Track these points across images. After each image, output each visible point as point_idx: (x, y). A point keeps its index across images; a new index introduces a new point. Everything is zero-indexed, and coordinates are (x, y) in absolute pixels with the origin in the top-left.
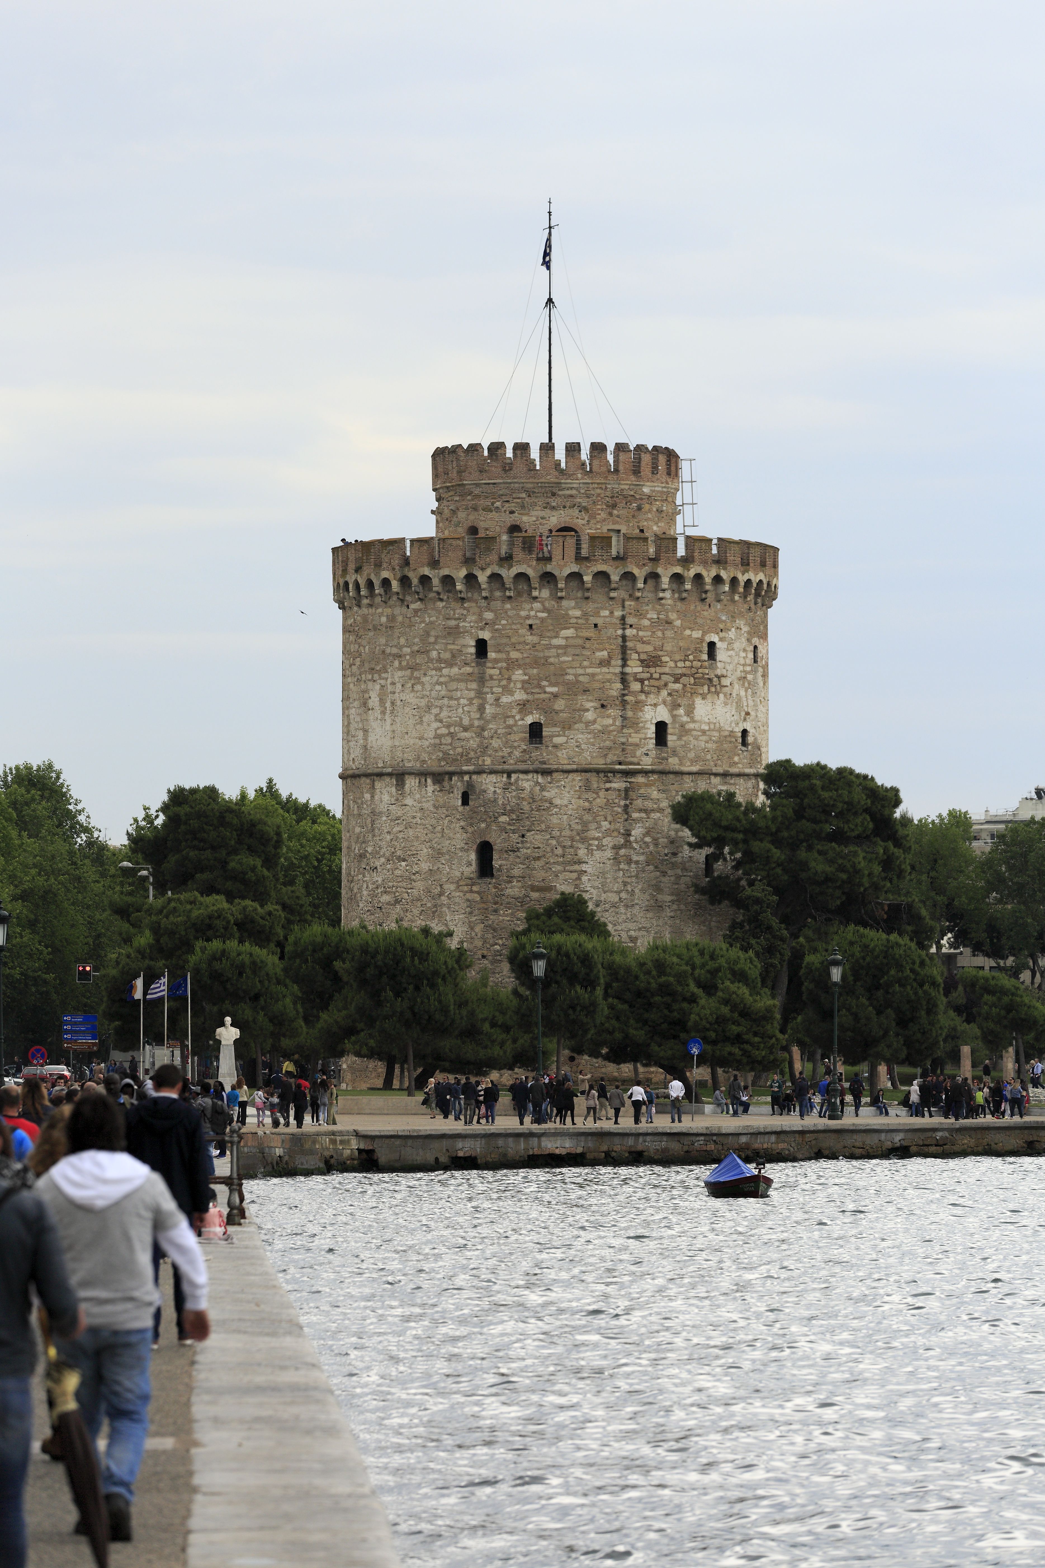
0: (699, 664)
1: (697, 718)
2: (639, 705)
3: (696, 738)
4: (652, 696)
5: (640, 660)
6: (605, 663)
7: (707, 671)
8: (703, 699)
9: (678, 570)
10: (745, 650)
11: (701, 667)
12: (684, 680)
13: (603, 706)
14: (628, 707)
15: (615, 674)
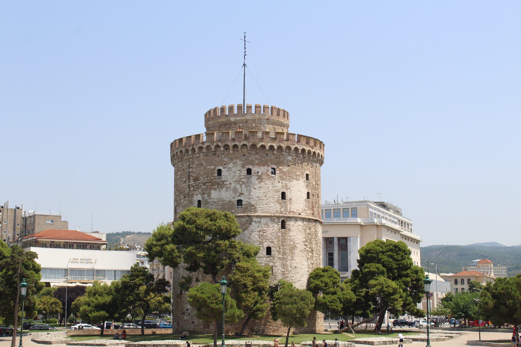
0: (213, 178)
1: (212, 198)
2: (193, 195)
3: (211, 205)
4: (196, 191)
5: (193, 179)
6: (185, 182)
7: (217, 180)
8: (215, 190)
9: (200, 145)
10: (239, 170)
11: (214, 179)
12: (207, 184)
13: (185, 197)
14: (190, 196)
15: (187, 185)
